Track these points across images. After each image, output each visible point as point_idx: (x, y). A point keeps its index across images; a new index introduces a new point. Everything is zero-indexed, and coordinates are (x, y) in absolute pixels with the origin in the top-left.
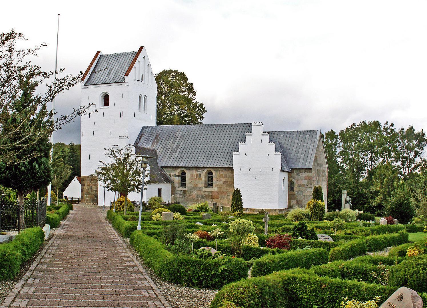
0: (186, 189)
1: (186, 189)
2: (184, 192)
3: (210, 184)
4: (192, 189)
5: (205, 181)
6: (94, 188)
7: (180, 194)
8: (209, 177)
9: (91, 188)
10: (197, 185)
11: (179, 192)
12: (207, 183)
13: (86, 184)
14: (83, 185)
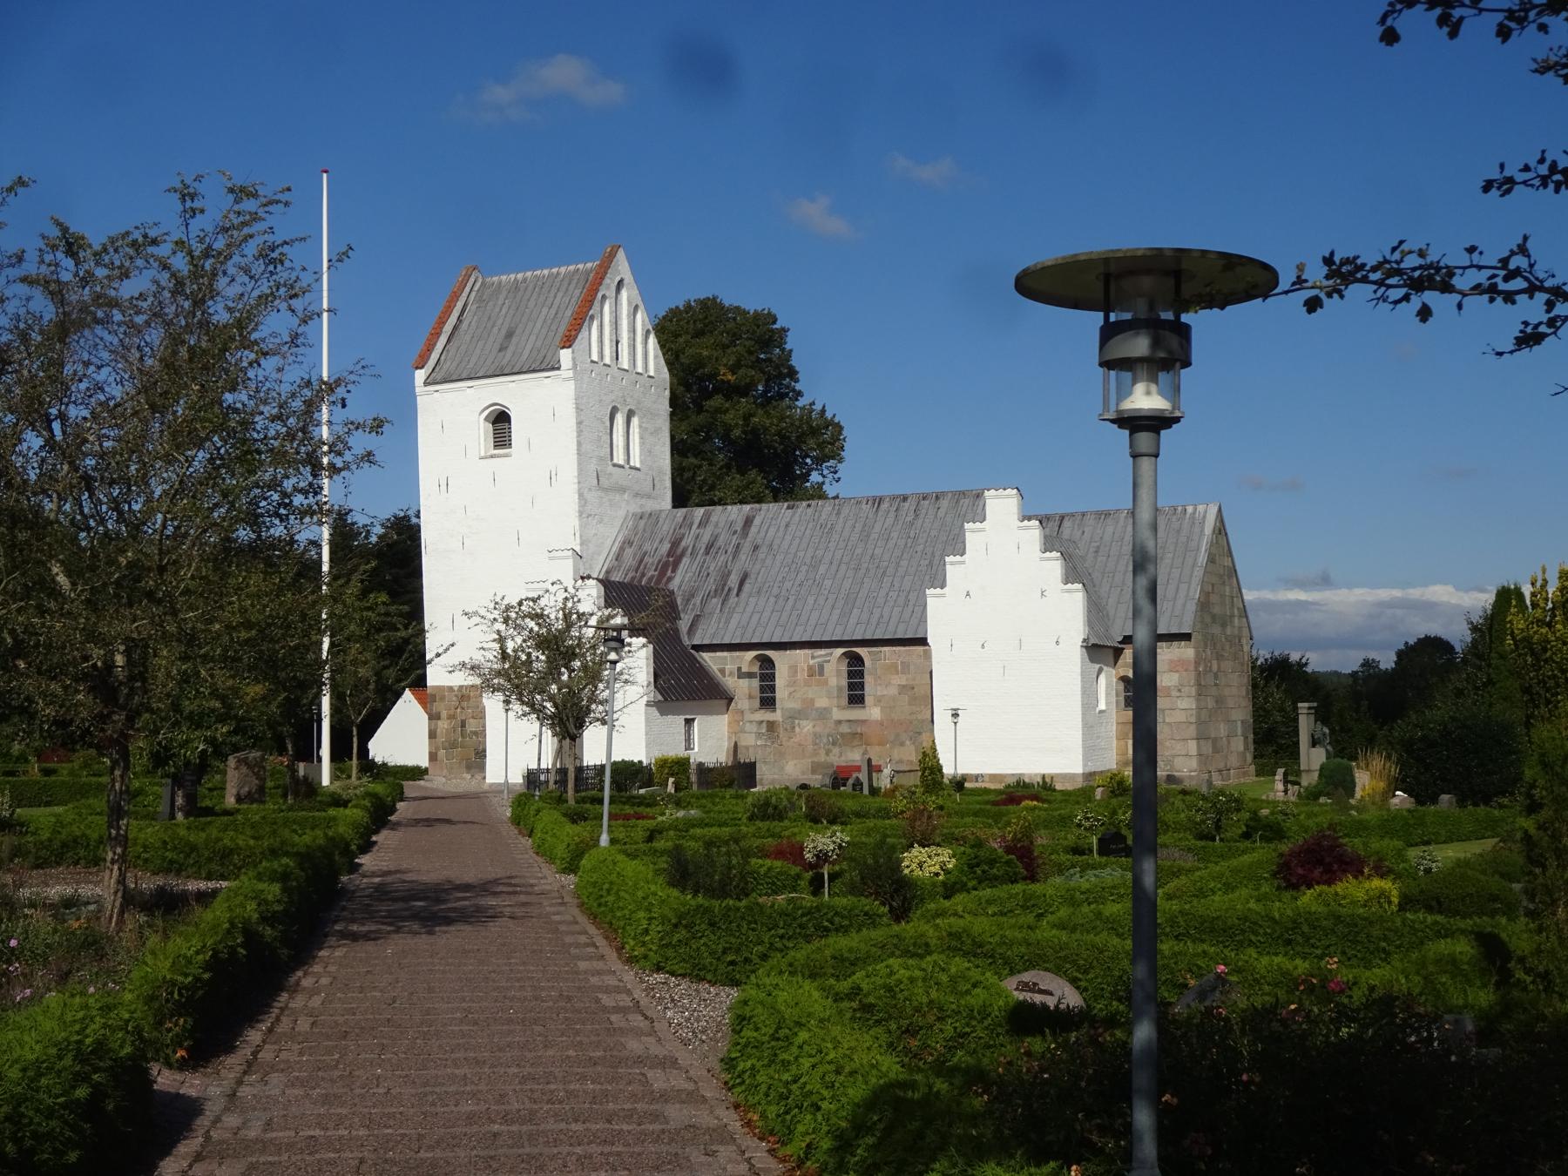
0: (777, 716)
1: (777, 716)
2: (771, 726)
3: (856, 697)
4: (793, 716)
5: (840, 689)
6: (472, 726)
7: (759, 735)
8: (851, 675)
9: (463, 725)
10: (812, 700)
11: (754, 728)
12: (846, 693)
13: (444, 714)
14: (434, 717)
